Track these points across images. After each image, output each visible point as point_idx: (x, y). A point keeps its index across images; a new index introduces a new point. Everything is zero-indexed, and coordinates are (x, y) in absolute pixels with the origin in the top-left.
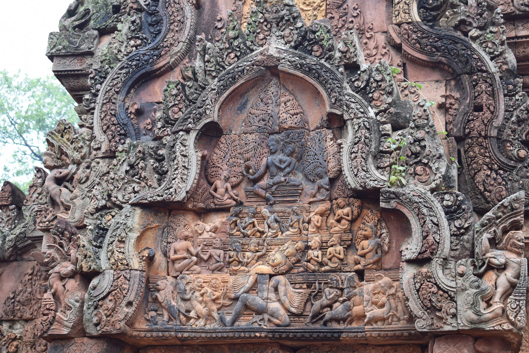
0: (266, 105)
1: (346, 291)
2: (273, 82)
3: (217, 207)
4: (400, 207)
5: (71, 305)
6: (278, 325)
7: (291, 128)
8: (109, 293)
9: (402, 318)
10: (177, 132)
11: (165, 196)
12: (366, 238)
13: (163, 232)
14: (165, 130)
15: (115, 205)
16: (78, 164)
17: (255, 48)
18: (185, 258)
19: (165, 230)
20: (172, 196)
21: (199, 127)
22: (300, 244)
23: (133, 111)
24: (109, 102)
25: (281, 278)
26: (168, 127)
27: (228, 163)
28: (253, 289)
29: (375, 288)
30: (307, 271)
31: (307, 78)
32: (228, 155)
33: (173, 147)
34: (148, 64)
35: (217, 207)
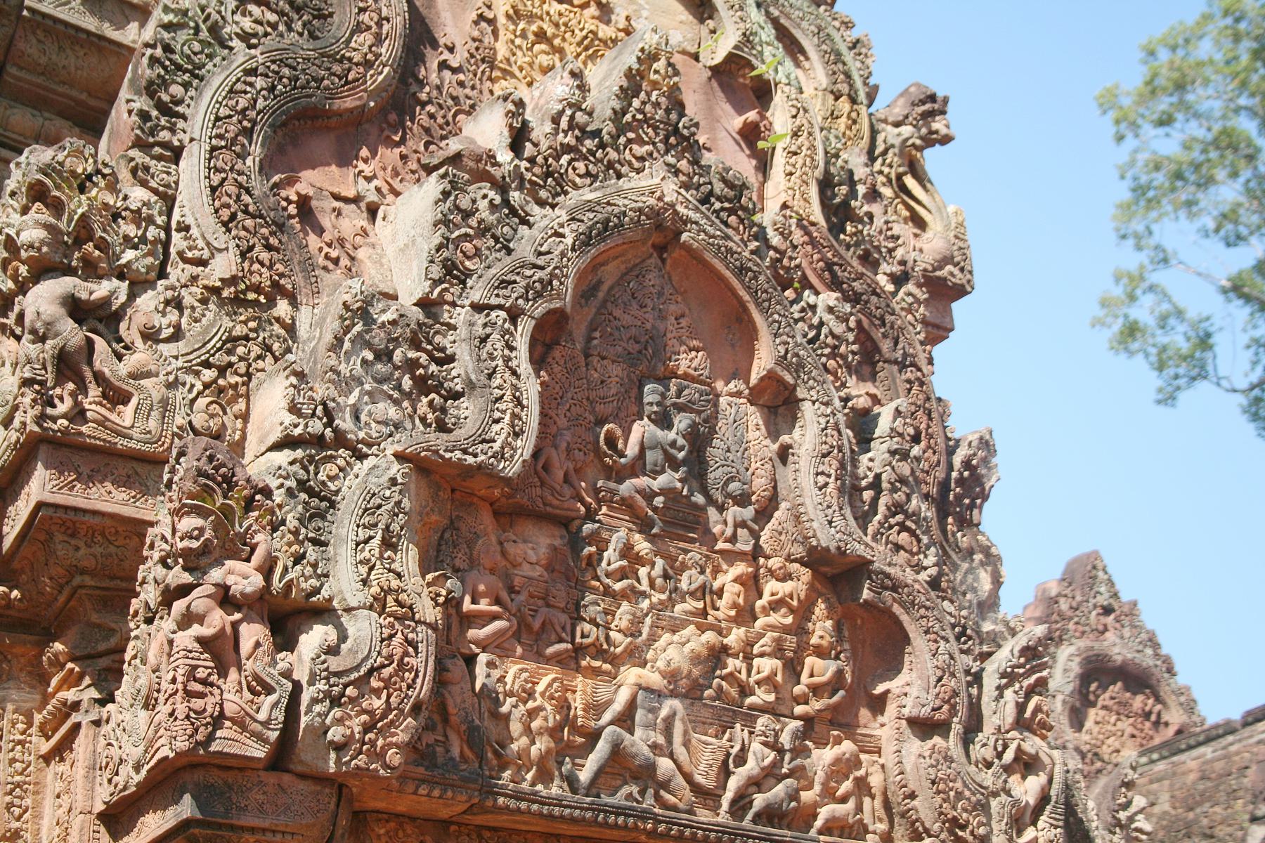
0: (641, 307)
1: (787, 757)
2: (652, 260)
3: (548, 509)
4: (896, 609)
5: (273, 684)
6: (674, 808)
7: (686, 376)
8: (371, 671)
9: (871, 828)
10: (492, 308)
11: (482, 458)
12: (820, 653)
13: (442, 537)
14: (446, 290)
15: (341, 440)
16: (138, 285)
17: (624, 170)
18: (495, 617)
19: (447, 535)
20: (499, 462)
21: (539, 312)
22: (710, 636)
23: (294, 198)
24: (225, 147)
25: (676, 703)
26: (452, 285)
27: (568, 414)
28: (626, 719)
29: (837, 761)
30: (718, 698)
31: (735, 283)
32: (570, 395)
33: (484, 340)
34: (318, 88)
35: (548, 509)
